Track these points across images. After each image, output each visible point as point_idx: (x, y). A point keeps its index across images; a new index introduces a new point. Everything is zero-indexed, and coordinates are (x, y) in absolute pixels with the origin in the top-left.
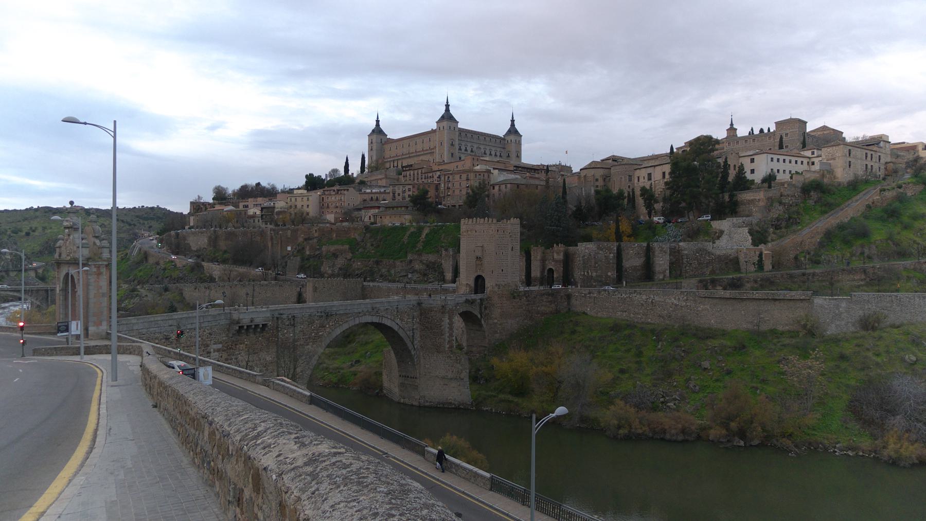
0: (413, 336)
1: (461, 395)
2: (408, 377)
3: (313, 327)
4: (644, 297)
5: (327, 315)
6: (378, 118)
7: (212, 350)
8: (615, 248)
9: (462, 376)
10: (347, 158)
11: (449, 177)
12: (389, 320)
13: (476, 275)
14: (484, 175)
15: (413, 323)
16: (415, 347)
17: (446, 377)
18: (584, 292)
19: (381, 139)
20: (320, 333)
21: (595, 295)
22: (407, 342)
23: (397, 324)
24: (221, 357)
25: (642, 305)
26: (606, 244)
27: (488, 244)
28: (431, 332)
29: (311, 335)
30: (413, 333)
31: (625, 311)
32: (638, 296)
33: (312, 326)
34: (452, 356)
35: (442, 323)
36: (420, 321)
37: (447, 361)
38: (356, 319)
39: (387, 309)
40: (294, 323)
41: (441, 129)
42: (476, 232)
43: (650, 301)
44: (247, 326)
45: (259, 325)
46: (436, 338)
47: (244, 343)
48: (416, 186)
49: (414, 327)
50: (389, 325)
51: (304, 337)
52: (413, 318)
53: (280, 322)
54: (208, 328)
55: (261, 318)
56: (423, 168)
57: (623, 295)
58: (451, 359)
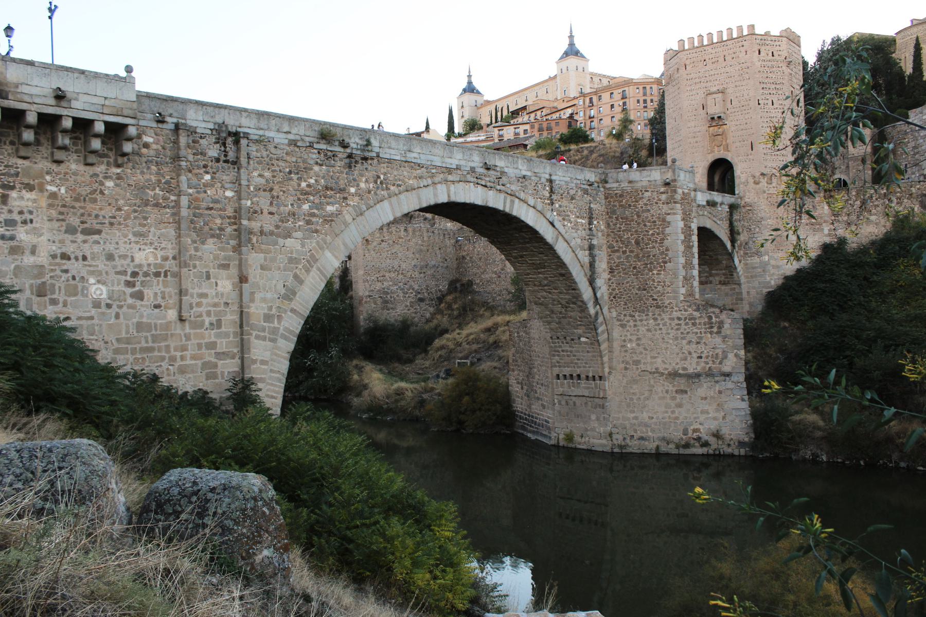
0: (592, 265)
1: (724, 418)
2: (579, 376)
3: (304, 184)
5: (350, 156)
6: (469, 72)
9: (726, 369)
11: (591, 99)
12: (531, 210)
13: (711, 158)
14: (651, 88)
15: (590, 229)
16: (599, 295)
17: (681, 372)
19: (476, 101)
20: (330, 208)
22: (577, 280)
23: (552, 224)
27: (737, 84)
28: (637, 256)
29: (299, 207)
30: (592, 256)
33: (300, 179)
34: (697, 314)
35: (668, 230)
36: (608, 226)
37: (683, 327)
38: (439, 186)
39: (524, 177)
40: (238, 158)
41: (564, 71)
44: (41, 116)
45: (90, 122)
46: (651, 270)
47: (42, 189)
48: (536, 126)
49: (595, 242)
50: (530, 222)
51: (274, 209)
52: (591, 219)
53: (183, 140)
55: (102, 101)
56: (543, 108)
58: (694, 324)
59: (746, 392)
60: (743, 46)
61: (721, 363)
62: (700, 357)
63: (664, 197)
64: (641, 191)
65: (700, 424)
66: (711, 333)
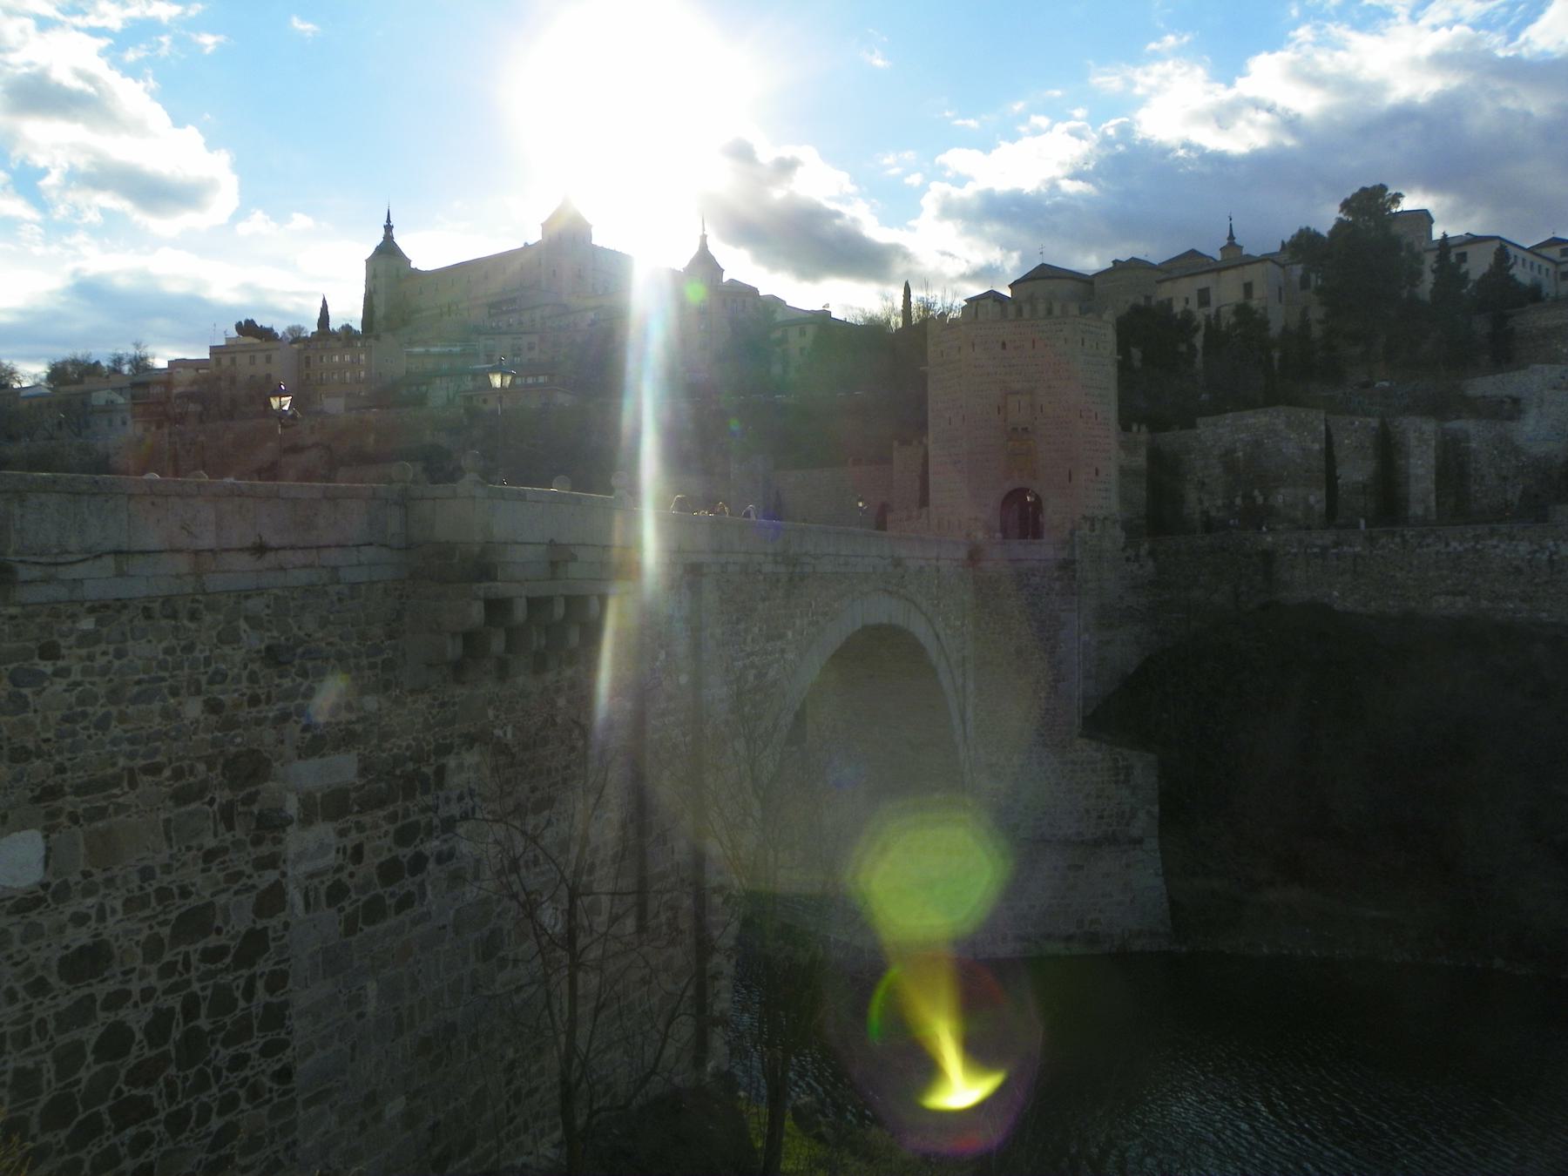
4: (1524, 548)
7: (292, 807)
8: (1323, 428)
10: (324, 302)
13: (1008, 486)
18: (1319, 542)
21: (1358, 549)
23: (938, 637)
24: (357, 854)
25: (1518, 570)
26: (1303, 415)
31: (1463, 593)
32: (1503, 546)
42: (1004, 345)
43: (1545, 557)
54: (255, 605)
57: (1454, 544)
59: (1160, 865)
60: (1061, 331)
61: (1128, 825)
62: (1101, 817)
63: (1057, 585)
64: (1026, 574)
65: (1100, 911)
66: (1116, 782)
